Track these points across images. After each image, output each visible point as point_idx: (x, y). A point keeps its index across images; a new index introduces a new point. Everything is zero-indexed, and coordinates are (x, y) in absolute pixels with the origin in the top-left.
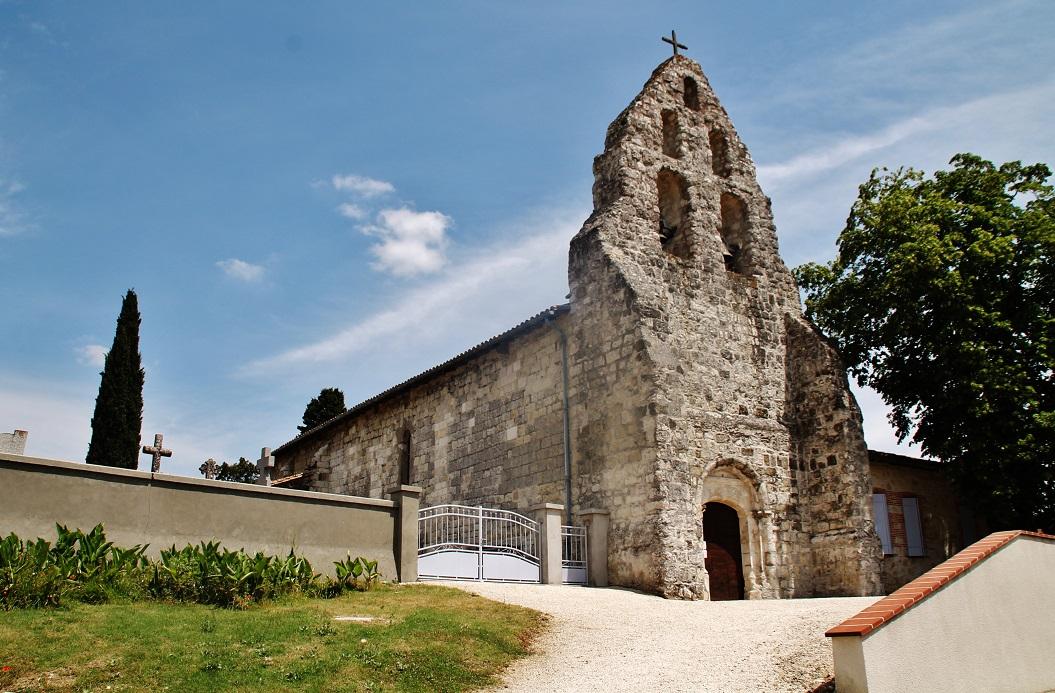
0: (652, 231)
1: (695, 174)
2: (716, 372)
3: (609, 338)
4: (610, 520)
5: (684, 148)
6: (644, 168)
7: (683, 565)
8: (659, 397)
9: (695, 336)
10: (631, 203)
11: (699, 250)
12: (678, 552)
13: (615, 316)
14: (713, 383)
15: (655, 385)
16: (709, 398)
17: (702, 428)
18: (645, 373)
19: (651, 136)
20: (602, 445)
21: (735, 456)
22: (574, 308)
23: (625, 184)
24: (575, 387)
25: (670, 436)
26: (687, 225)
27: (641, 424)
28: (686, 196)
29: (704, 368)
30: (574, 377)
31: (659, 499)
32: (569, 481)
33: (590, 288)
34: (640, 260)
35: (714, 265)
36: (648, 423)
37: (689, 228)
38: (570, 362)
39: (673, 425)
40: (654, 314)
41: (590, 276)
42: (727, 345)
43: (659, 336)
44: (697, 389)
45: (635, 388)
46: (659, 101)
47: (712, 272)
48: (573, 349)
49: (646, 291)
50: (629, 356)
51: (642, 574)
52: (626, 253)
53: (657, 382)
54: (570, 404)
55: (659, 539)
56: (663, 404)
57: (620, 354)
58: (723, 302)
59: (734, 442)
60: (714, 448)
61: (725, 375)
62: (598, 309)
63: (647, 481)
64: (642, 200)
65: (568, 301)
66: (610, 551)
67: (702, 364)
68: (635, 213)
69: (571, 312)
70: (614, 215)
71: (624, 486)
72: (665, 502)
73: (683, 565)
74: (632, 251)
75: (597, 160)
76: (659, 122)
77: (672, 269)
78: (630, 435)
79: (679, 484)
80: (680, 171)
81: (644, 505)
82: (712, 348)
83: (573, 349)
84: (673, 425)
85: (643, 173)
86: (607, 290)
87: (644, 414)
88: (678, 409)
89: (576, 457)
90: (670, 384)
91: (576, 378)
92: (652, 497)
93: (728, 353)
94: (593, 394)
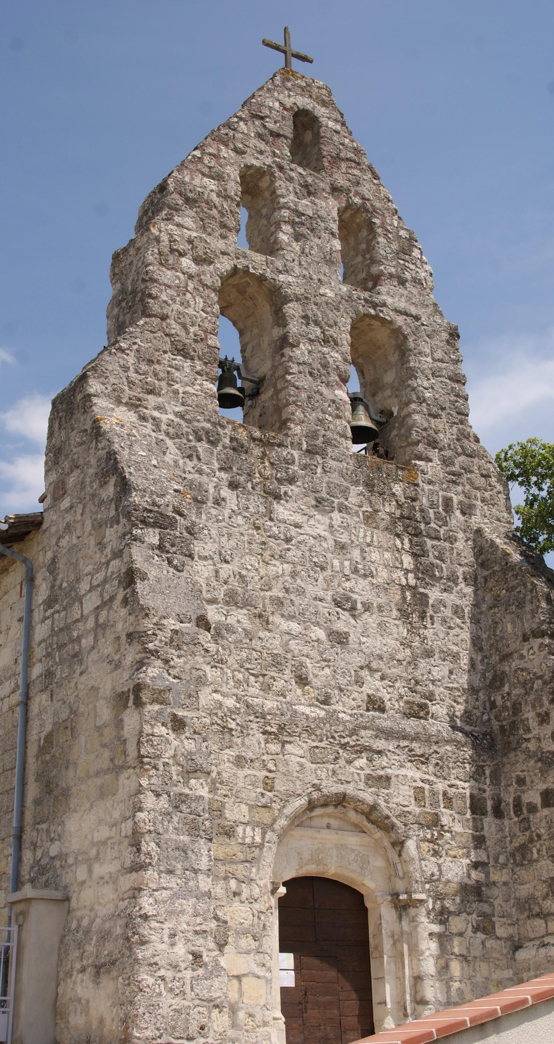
0: (200, 380)
1: (301, 281)
2: (321, 634)
3: (89, 568)
4: (69, 912)
5: (284, 236)
6: (194, 268)
7: (178, 1002)
8: (153, 671)
9: (278, 567)
10: (161, 329)
11: (299, 414)
12: (170, 975)
13: (99, 526)
14: (314, 654)
15: (146, 650)
16: (302, 681)
17: (280, 734)
18: (131, 629)
19: (214, 212)
20: (67, 768)
21: (350, 789)
22: (50, 517)
23: (150, 296)
24: (40, 661)
25: (173, 746)
26: (279, 373)
27: (119, 724)
28: (280, 320)
29: (294, 627)
30: (40, 643)
31: (138, 867)
32: (19, 838)
33: (71, 480)
34: (171, 430)
35: (328, 442)
36: (130, 719)
37: (283, 377)
38: (37, 616)
39: (178, 725)
40: (162, 522)
41: (73, 460)
42: (348, 584)
43: (170, 562)
44: (277, 662)
45: (117, 657)
46: (236, 150)
47: (324, 455)
48: (42, 592)
49: (155, 482)
50: (112, 599)
51: (101, 1021)
52: (143, 418)
53: (151, 646)
54: (31, 694)
55: (130, 949)
56: (160, 685)
57: (101, 595)
58: (342, 509)
59: (349, 762)
60: (301, 768)
61: (339, 639)
62: (79, 517)
63: (123, 834)
64: (184, 326)
65: (40, 508)
66: (62, 975)
67: (291, 617)
68: (168, 347)
69: (45, 526)
70: (122, 351)
71: (93, 844)
72: (151, 873)
73: (178, 1002)
74: (156, 414)
75: (116, 257)
76: (234, 188)
77: (238, 447)
78: (104, 746)
79: (185, 838)
80: (269, 274)
81: (115, 881)
82: (311, 590)
83: (42, 592)
84: (178, 725)
85: (191, 277)
86: (91, 482)
87: (126, 707)
88: (193, 696)
89: (33, 791)
90: (178, 648)
91: (43, 645)
92: (128, 864)
93: (348, 599)
94: (62, 671)
